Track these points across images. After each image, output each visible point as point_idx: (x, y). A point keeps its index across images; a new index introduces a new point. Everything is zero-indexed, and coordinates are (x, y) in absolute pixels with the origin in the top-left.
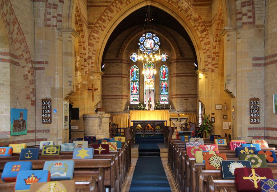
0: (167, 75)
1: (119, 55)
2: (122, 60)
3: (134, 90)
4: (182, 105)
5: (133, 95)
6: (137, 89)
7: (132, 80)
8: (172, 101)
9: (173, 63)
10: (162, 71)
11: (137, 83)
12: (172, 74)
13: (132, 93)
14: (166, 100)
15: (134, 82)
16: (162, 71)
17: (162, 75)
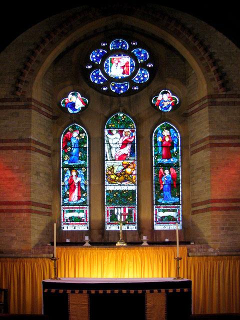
0: (175, 150)
1: (19, 85)
2: (30, 100)
3: (74, 190)
4: (230, 232)
5: (68, 204)
6: (83, 187)
7: (66, 163)
8: (194, 225)
9: (196, 111)
10: (160, 139)
11: (81, 172)
12: (193, 145)
13: (66, 201)
14: (174, 219)
15: (71, 168)
16: (160, 139)
17: (160, 149)
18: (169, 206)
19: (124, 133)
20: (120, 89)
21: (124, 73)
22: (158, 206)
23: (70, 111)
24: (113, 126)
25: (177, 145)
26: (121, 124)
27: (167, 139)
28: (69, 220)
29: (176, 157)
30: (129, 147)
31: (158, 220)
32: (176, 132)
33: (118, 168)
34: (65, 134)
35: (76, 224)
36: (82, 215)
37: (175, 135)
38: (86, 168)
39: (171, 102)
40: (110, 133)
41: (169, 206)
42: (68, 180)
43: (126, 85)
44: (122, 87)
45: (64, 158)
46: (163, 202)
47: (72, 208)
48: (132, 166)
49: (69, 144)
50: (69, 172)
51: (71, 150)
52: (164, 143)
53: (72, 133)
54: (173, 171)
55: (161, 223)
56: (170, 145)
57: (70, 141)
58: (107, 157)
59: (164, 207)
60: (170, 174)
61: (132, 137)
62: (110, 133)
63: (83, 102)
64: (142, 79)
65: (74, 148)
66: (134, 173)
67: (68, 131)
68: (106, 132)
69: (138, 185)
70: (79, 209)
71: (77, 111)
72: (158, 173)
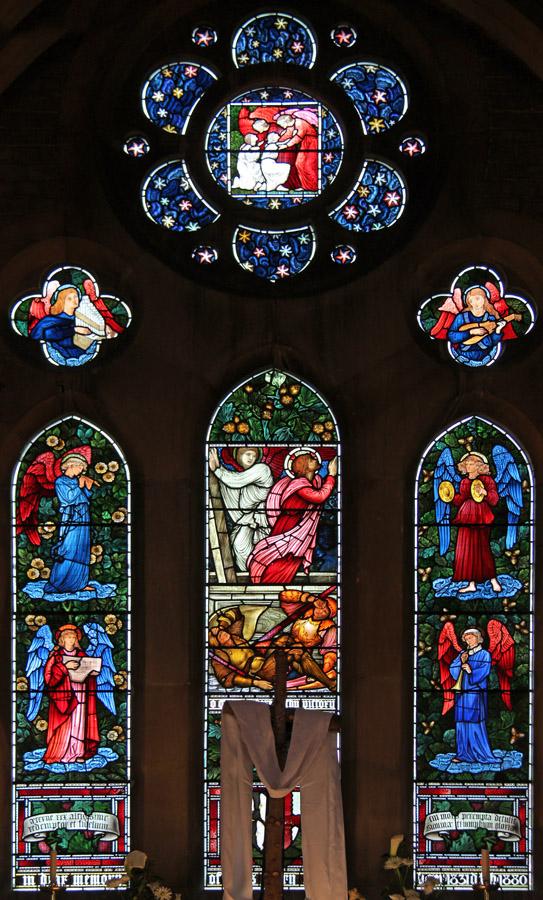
3: (69, 713)
6: (109, 701)
7: (35, 591)
10: (445, 492)
13: (34, 760)
14: (501, 846)
15: (57, 618)
16: (445, 492)
17: (445, 535)
18: (481, 786)
19: (288, 463)
20: (275, 259)
21: (292, 183)
22: (432, 785)
23: (53, 356)
24: (242, 428)
25: (522, 520)
26: (277, 422)
27: (478, 494)
28: (43, 847)
29: (514, 571)
30: (308, 525)
31: (428, 847)
32: (519, 461)
33: (259, 621)
34: (28, 462)
35: (75, 863)
36: (101, 822)
37: (516, 476)
38: (122, 616)
39: (502, 325)
40: (232, 462)
41: (481, 786)
42: (43, 668)
43: (303, 239)
44: (286, 251)
45: (23, 571)
46: (454, 769)
47: (61, 792)
48: (320, 611)
49: (46, 506)
50: (46, 632)
51: (56, 534)
52: (464, 508)
53: (59, 457)
54: (494, 627)
55: (444, 862)
56: (489, 519)
57: (52, 494)
58: (213, 568)
59: (455, 792)
60: (485, 645)
61: (324, 480)
62: (232, 462)
63: (111, 318)
64: (374, 210)
65: (67, 524)
66: (329, 642)
67: (41, 447)
68: (212, 457)
69: (347, 695)
70: (88, 798)
71: (83, 359)
72: (435, 643)
